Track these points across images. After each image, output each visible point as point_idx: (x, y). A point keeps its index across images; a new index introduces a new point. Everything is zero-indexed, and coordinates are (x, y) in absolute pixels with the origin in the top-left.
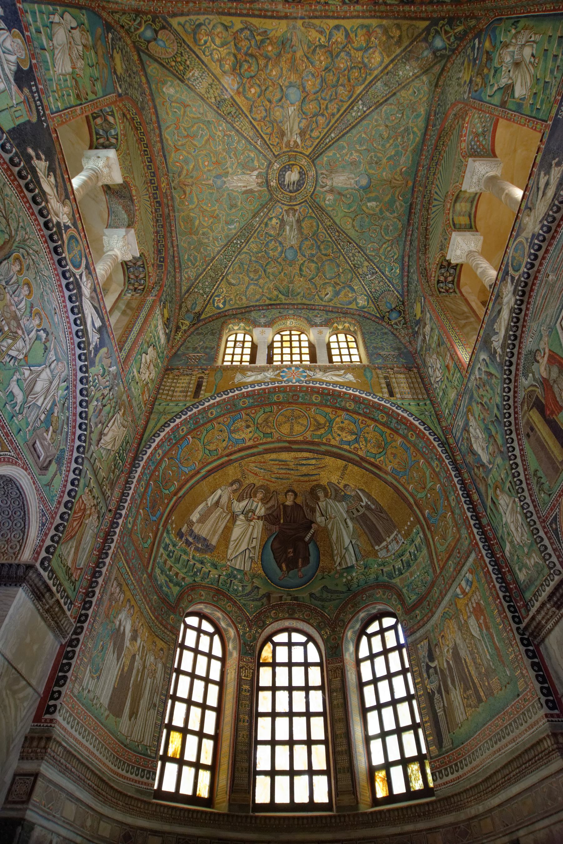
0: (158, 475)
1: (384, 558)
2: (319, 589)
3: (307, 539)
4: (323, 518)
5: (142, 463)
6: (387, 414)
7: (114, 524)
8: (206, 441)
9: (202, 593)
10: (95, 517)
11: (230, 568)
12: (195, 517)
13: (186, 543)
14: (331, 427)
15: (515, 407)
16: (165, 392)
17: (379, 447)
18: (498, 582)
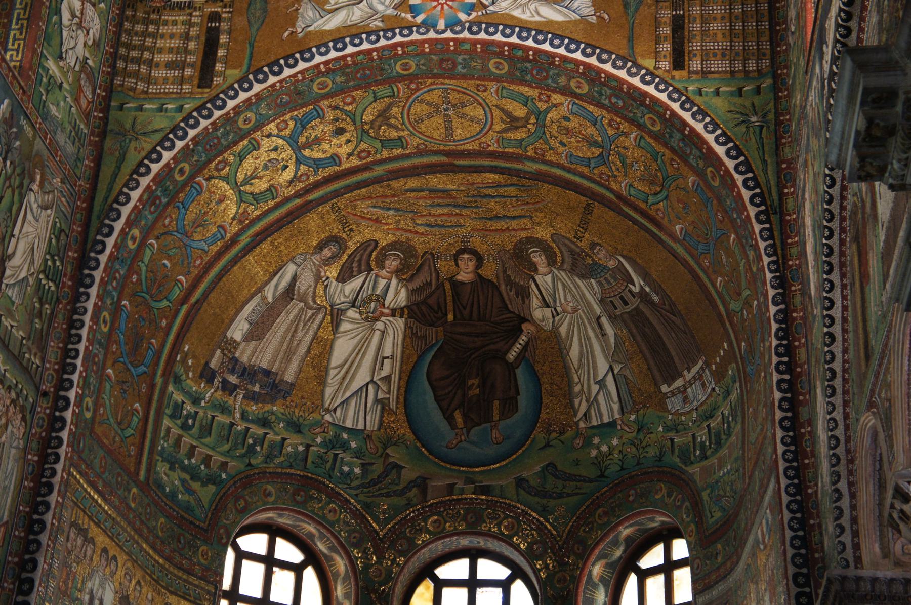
0: (139, 280)
1: (676, 413)
2: (538, 469)
3: (512, 356)
4: (548, 312)
5: (98, 275)
6: (662, 116)
7: (56, 423)
8: (241, 176)
9: (269, 487)
10: (17, 422)
11: (331, 428)
12: (238, 330)
13: (224, 389)
14: (541, 125)
15: (843, 219)
16: (132, 67)
17: (652, 183)
18: (792, 545)
